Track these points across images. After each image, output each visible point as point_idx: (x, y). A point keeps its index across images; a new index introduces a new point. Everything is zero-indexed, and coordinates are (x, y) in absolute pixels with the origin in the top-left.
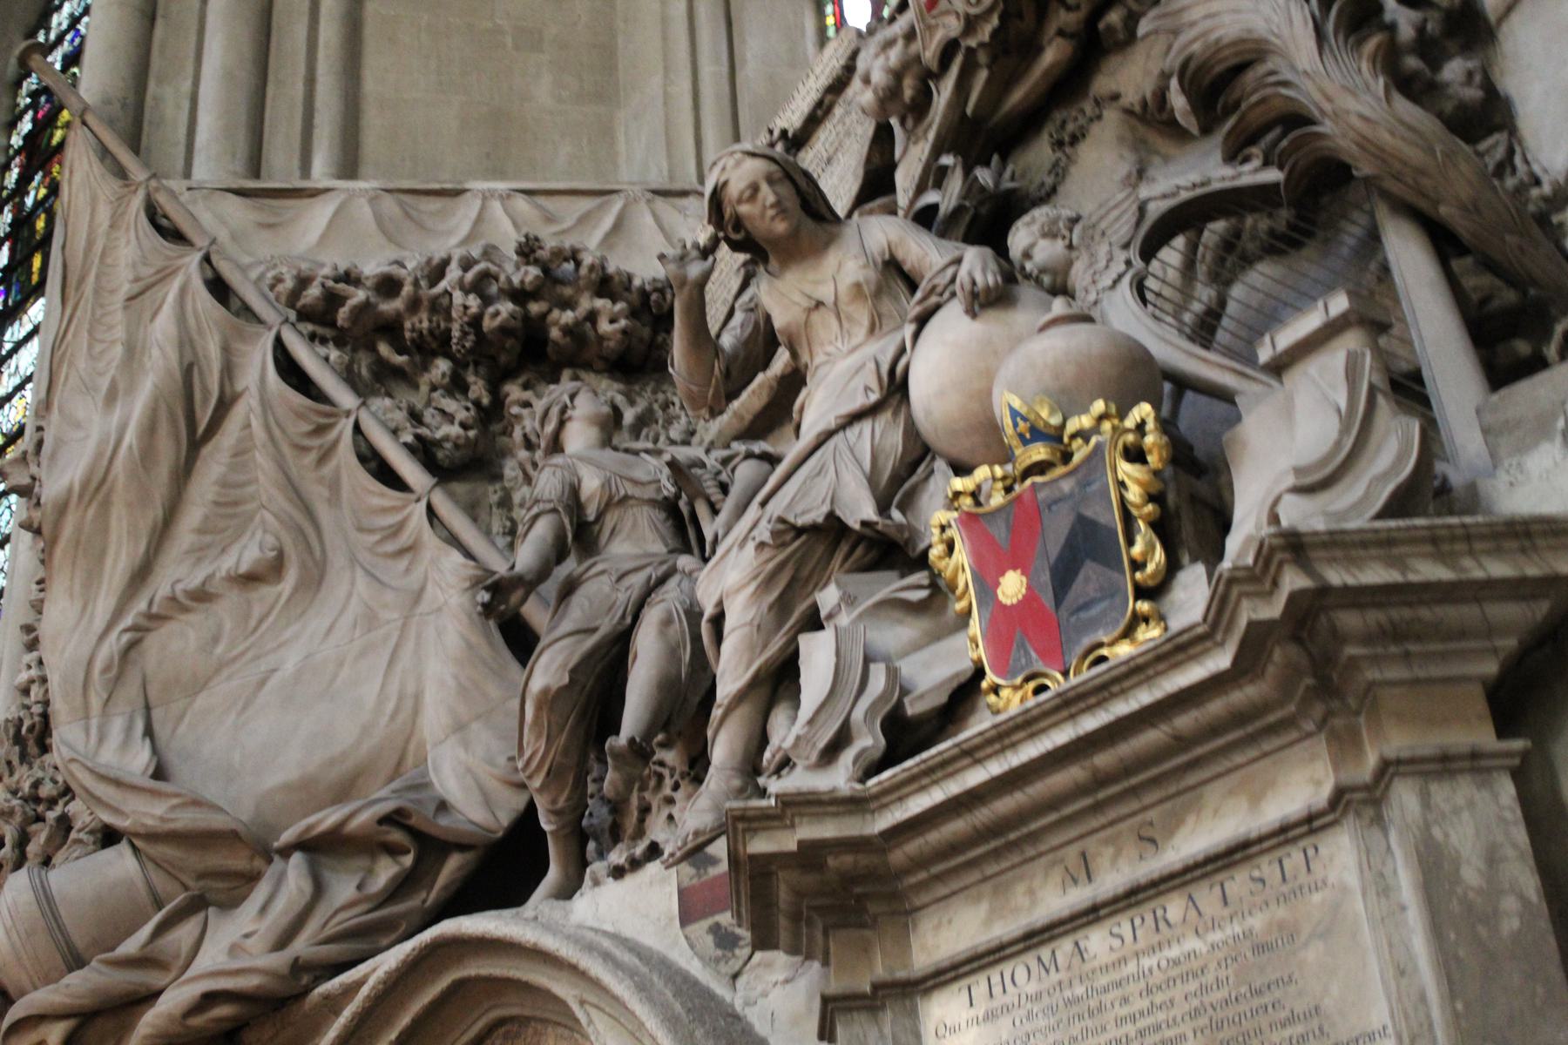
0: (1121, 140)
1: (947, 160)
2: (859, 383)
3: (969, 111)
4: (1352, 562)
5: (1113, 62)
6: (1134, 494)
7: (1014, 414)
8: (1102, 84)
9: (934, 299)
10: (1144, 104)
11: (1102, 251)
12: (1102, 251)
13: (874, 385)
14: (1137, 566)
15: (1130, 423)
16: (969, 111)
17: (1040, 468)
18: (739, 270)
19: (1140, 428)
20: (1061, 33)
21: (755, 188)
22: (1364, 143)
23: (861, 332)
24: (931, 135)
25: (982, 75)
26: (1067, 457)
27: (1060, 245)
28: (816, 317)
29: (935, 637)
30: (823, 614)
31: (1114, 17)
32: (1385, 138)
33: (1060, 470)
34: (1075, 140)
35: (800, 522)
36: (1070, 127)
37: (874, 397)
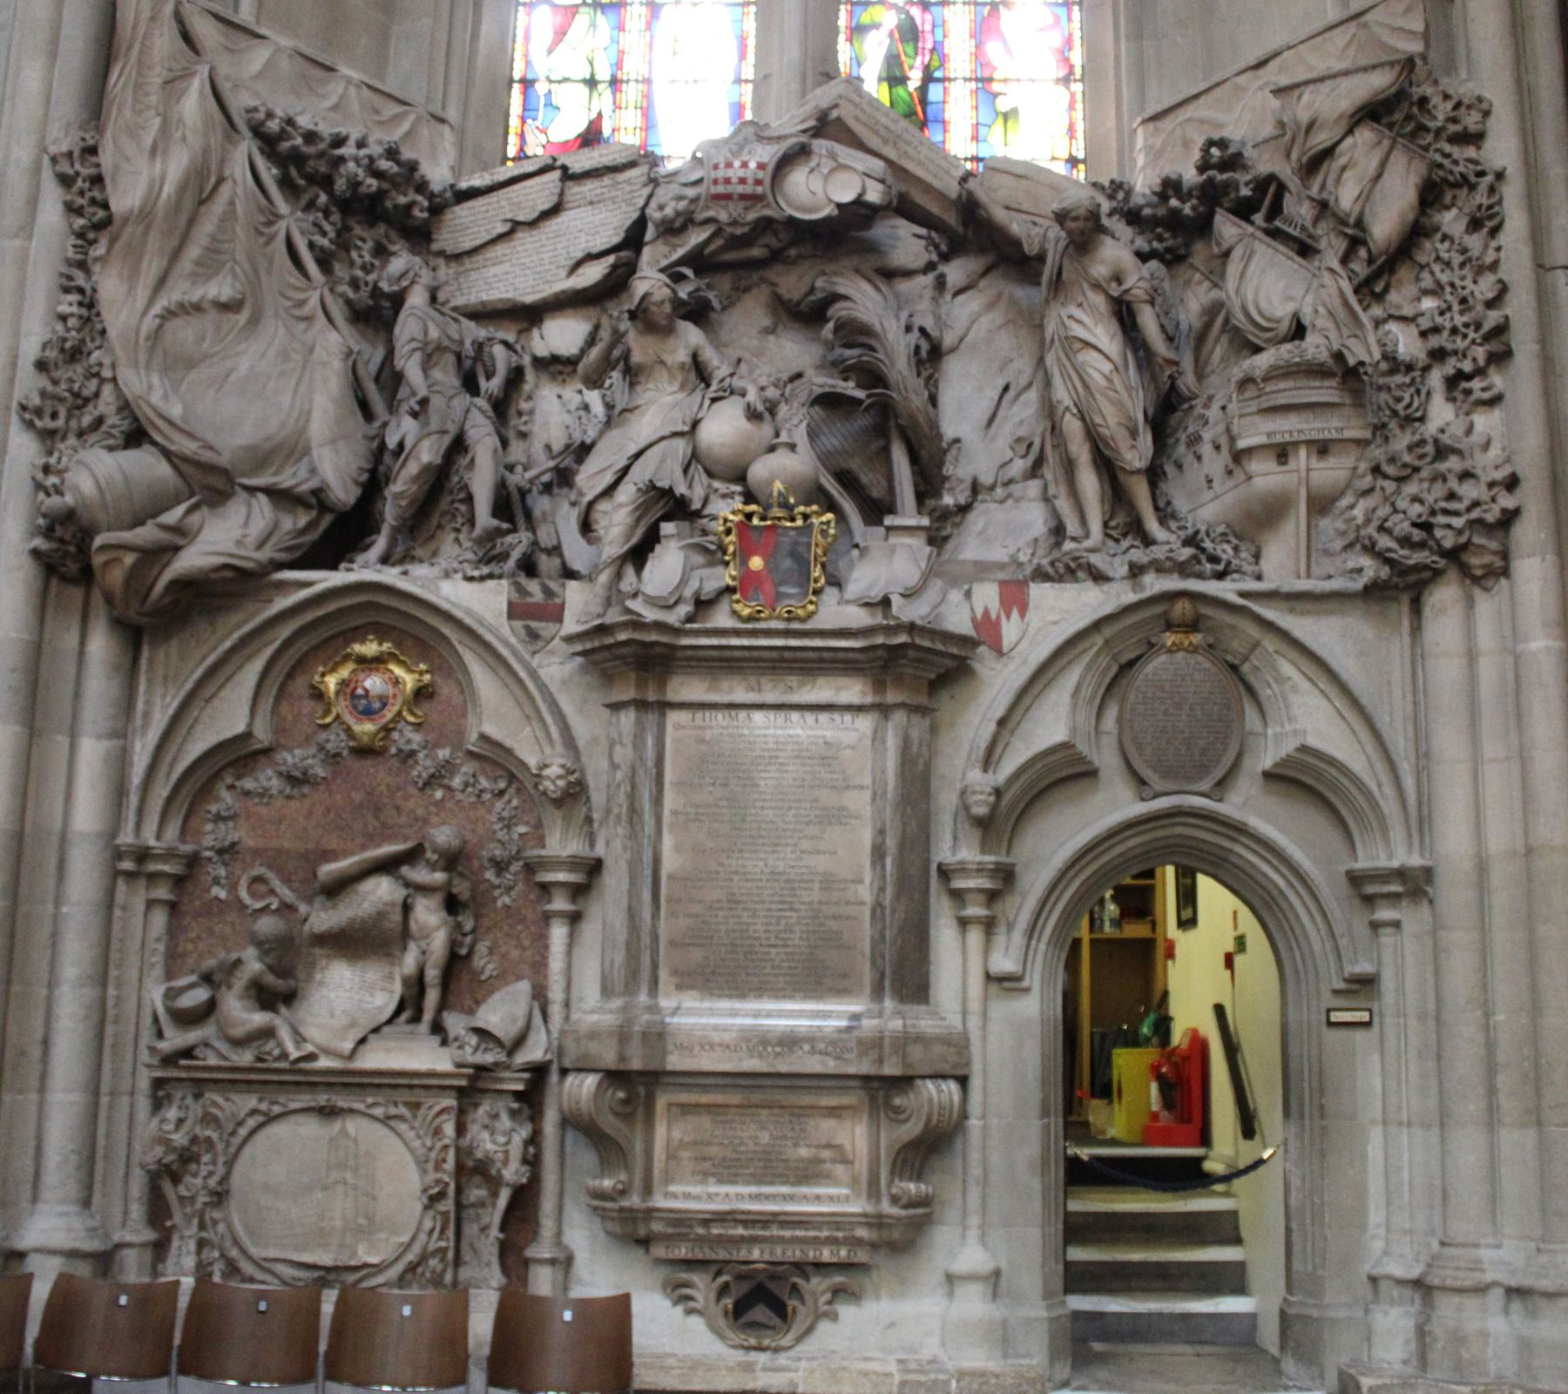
0: (768, 306)
1: (688, 272)
2: (677, 414)
3: (707, 251)
4: (922, 637)
5: (779, 267)
6: (819, 551)
7: (780, 493)
8: (771, 274)
9: (721, 394)
10: (790, 301)
11: (796, 405)
12: (796, 405)
13: (689, 422)
14: (816, 581)
15: (824, 519)
16: (707, 251)
17: (779, 519)
18: (506, 221)
19: (828, 523)
20: (766, 246)
21: (662, 302)
22: (912, 416)
23: (676, 386)
24: (680, 252)
25: (719, 242)
26: (793, 519)
27: (778, 393)
28: (657, 367)
29: (711, 564)
30: (663, 532)
31: (793, 252)
32: (921, 419)
33: (788, 524)
34: (747, 290)
35: (659, 484)
36: (743, 283)
37: (686, 429)
